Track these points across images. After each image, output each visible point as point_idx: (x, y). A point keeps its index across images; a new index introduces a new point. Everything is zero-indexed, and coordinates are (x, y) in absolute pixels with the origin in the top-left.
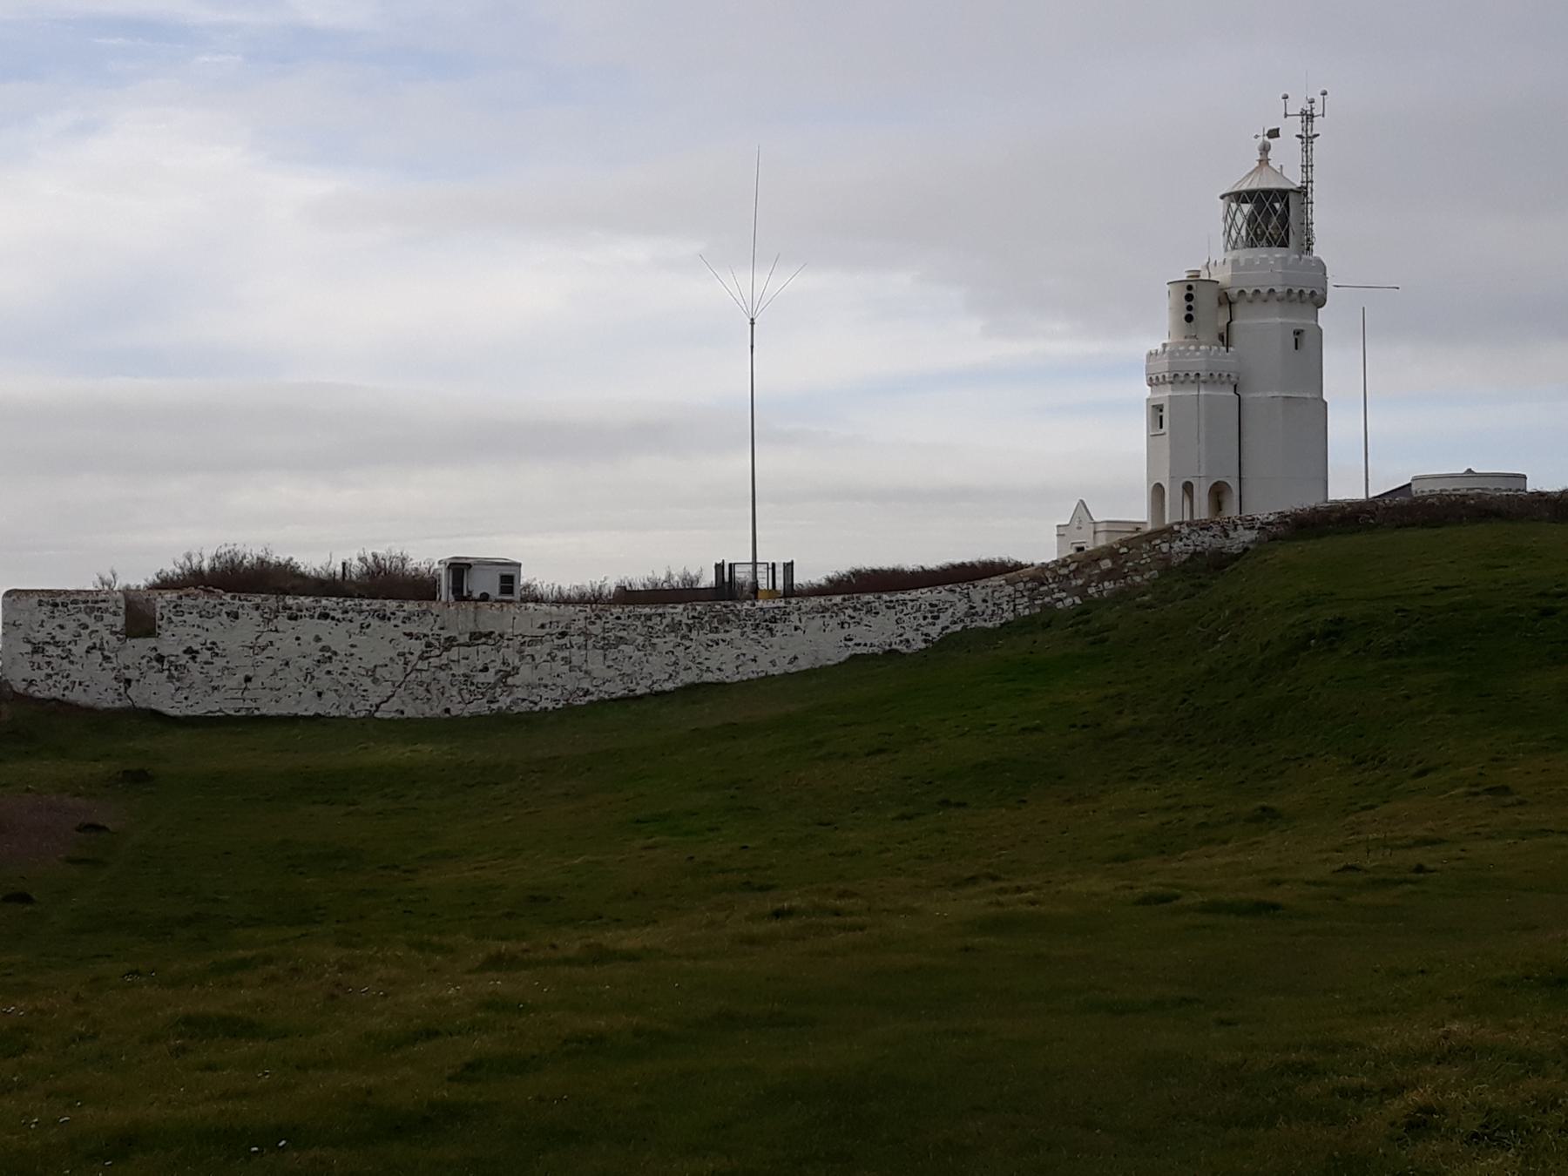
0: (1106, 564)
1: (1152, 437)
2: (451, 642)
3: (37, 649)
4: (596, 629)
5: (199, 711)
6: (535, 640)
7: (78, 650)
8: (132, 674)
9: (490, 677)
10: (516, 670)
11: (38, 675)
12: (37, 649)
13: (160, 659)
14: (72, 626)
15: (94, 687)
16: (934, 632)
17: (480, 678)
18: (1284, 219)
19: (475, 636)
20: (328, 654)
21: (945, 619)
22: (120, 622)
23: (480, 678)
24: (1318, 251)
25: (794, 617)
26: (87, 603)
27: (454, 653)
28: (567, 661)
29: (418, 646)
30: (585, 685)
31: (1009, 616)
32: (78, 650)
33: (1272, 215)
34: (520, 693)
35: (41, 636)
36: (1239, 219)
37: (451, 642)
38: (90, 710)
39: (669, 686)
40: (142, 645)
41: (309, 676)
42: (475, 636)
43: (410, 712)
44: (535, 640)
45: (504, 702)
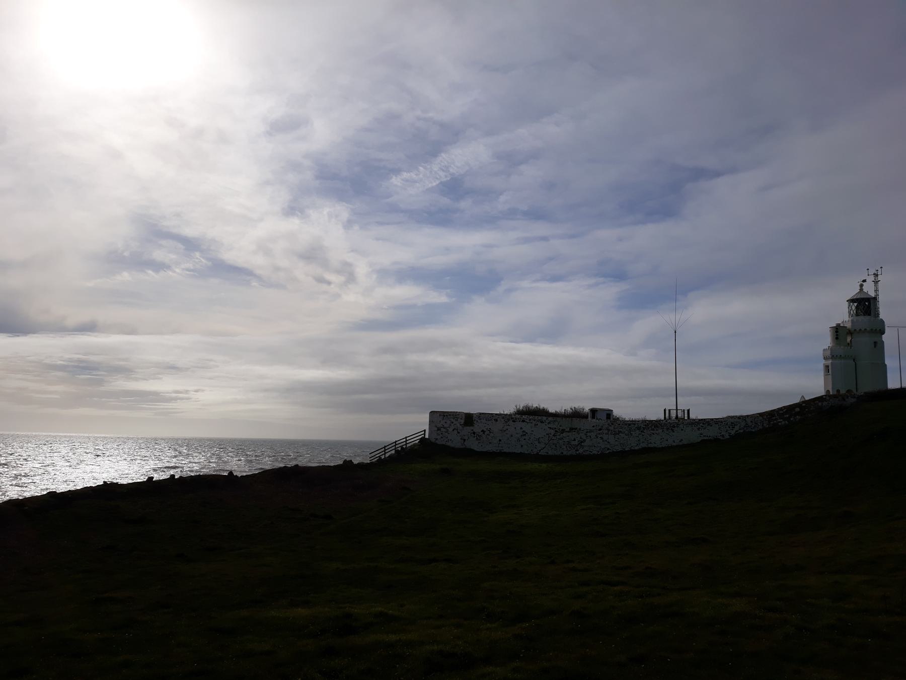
0: (797, 409)
1: (825, 375)
2: (563, 431)
3: (439, 429)
4: (612, 428)
5: (485, 450)
6: (591, 431)
7: (450, 430)
8: (466, 438)
9: (576, 443)
10: (585, 441)
11: (439, 437)
12: (439, 429)
13: (474, 433)
14: (449, 422)
15: (454, 441)
16: (733, 432)
17: (573, 443)
18: (869, 306)
19: (571, 429)
20: (524, 434)
21: (737, 428)
22: (463, 421)
23: (573, 443)
24: (881, 316)
25: (681, 426)
26: (454, 415)
27: (564, 434)
28: (602, 438)
29: (553, 432)
30: (608, 446)
31: (761, 427)
32: (450, 430)
33: (865, 305)
34: (586, 448)
35: (439, 425)
36: (854, 308)
37: (563, 431)
38: (453, 448)
39: (636, 448)
40: (468, 429)
41: (519, 440)
42: (571, 429)
43: (550, 453)
44: (591, 431)
45: (581, 451)
